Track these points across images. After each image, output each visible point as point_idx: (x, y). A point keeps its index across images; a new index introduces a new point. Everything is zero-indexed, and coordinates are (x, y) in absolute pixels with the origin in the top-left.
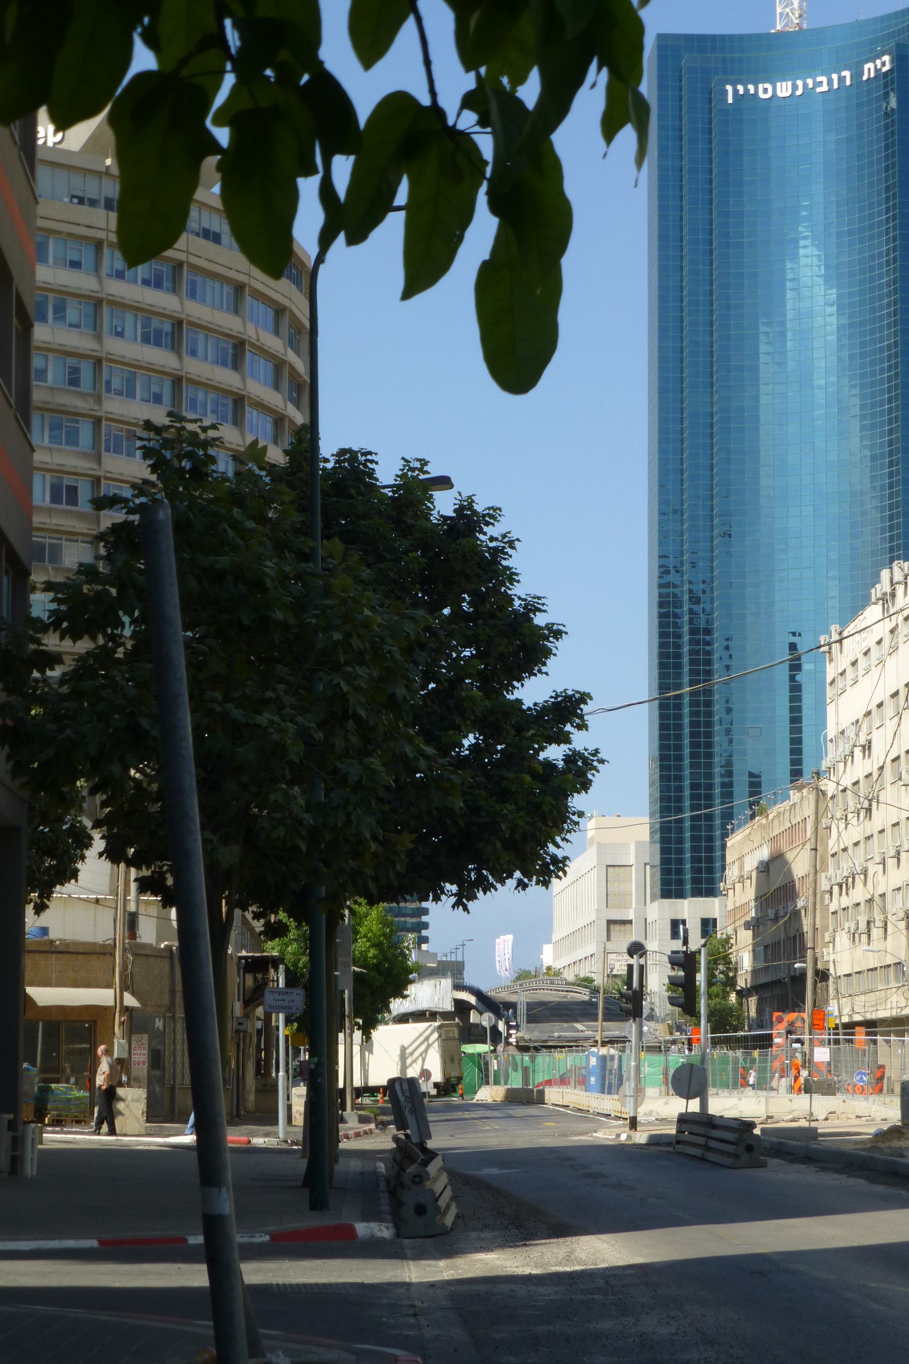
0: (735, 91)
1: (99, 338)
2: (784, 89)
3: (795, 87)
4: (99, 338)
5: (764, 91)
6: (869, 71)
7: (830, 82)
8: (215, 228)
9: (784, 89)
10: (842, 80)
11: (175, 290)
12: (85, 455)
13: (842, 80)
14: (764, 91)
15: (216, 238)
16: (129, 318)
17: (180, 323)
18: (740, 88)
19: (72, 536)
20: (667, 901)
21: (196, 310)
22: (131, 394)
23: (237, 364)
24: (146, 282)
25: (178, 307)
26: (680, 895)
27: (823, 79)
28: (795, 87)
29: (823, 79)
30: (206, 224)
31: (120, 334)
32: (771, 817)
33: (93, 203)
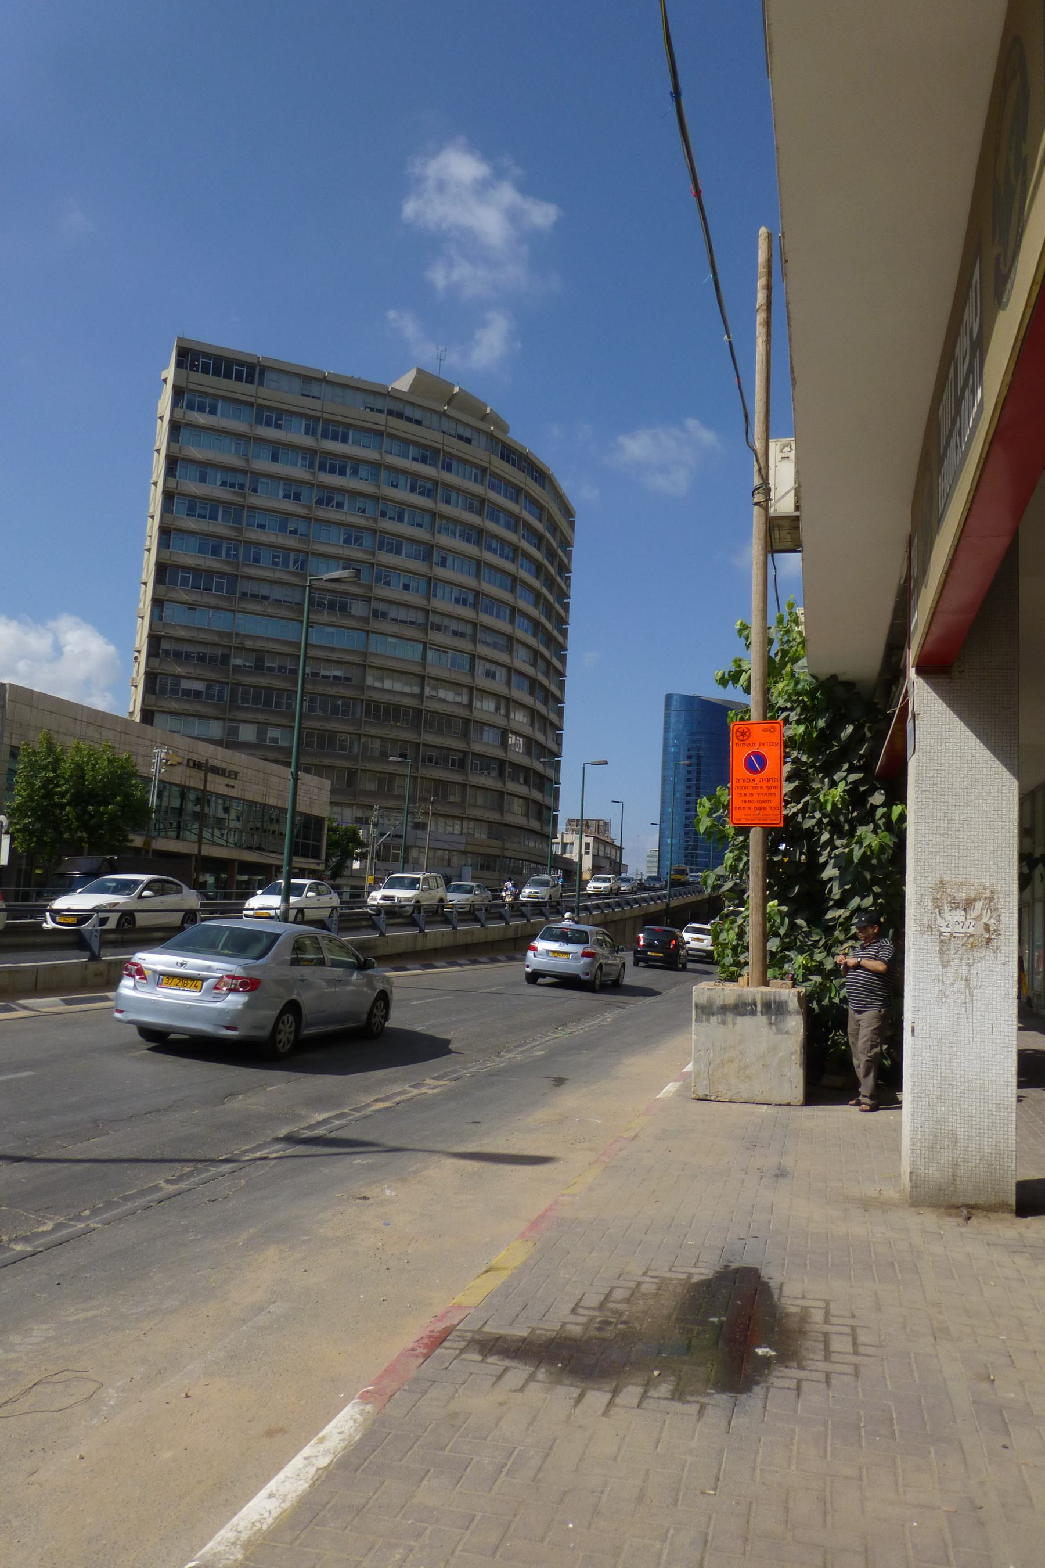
1: (378, 487)
4: (378, 487)
8: (467, 434)
11: (434, 465)
12: (365, 551)
15: (469, 441)
16: (402, 480)
17: (437, 483)
19: (355, 597)
22: (400, 519)
23: (480, 513)
24: (414, 459)
25: (436, 475)
30: (461, 430)
31: (396, 486)
33: (380, 411)
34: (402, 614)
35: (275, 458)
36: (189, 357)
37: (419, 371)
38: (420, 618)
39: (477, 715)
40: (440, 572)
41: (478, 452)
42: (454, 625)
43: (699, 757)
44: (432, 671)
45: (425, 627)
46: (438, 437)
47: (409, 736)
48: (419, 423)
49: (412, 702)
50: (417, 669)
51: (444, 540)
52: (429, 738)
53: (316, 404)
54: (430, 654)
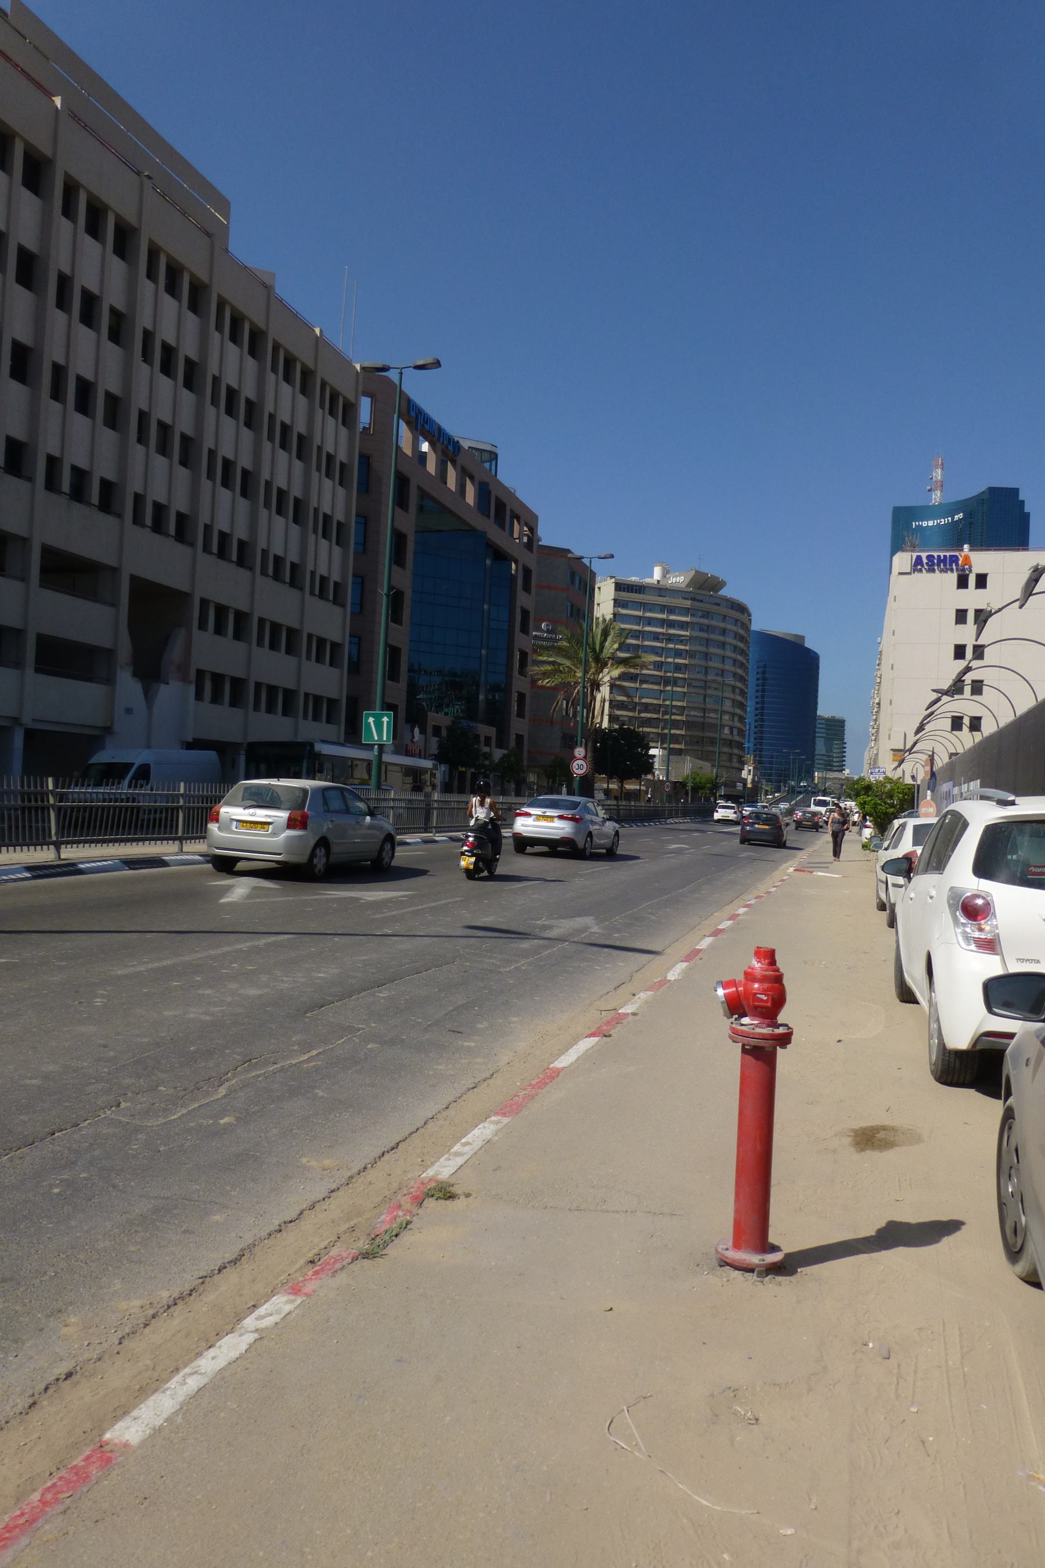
2: (931, 523)
5: (925, 524)
6: (956, 517)
9: (931, 523)
14: (925, 524)
21: (714, 623)
35: (649, 624)
36: (619, 587)
37: (696, 572)
38: (702, 684)
39: (724, 722)
40: (711, 664)
41: (723, 610)
42: (715, 685)
43: (764, 679)
44: (709, 706)
45: (705, 688)
46: (709, 606)
47: (700, 734)
48: (701, 601)
49: (701, 720)
50: (703, 706)
51: (712, 650)
52: (707, 734)
53: (665, 599)
54: (707, 700)
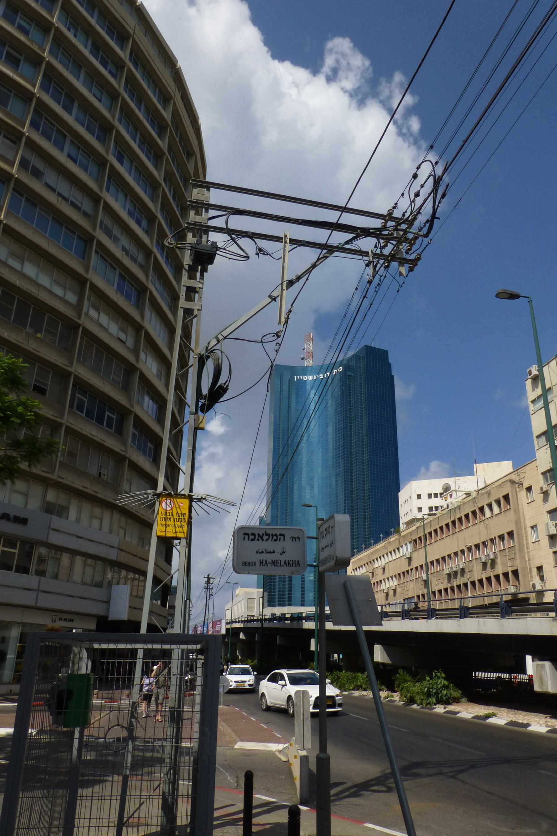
0: (297, 378)
2: (310, 378)
3: (313, 377)
5: (305, 378)
7: (324, 376)
9: (310, 378)
10: (327, 375)
13: (327, 375)
14: (305, 378)
18: (298, 377)
20: (270, 608)
26: (274, 606)
27: (322, 375)
28: (313, 377)
29: (322, 375)
32: (402, 534)
34: (64, 187)
